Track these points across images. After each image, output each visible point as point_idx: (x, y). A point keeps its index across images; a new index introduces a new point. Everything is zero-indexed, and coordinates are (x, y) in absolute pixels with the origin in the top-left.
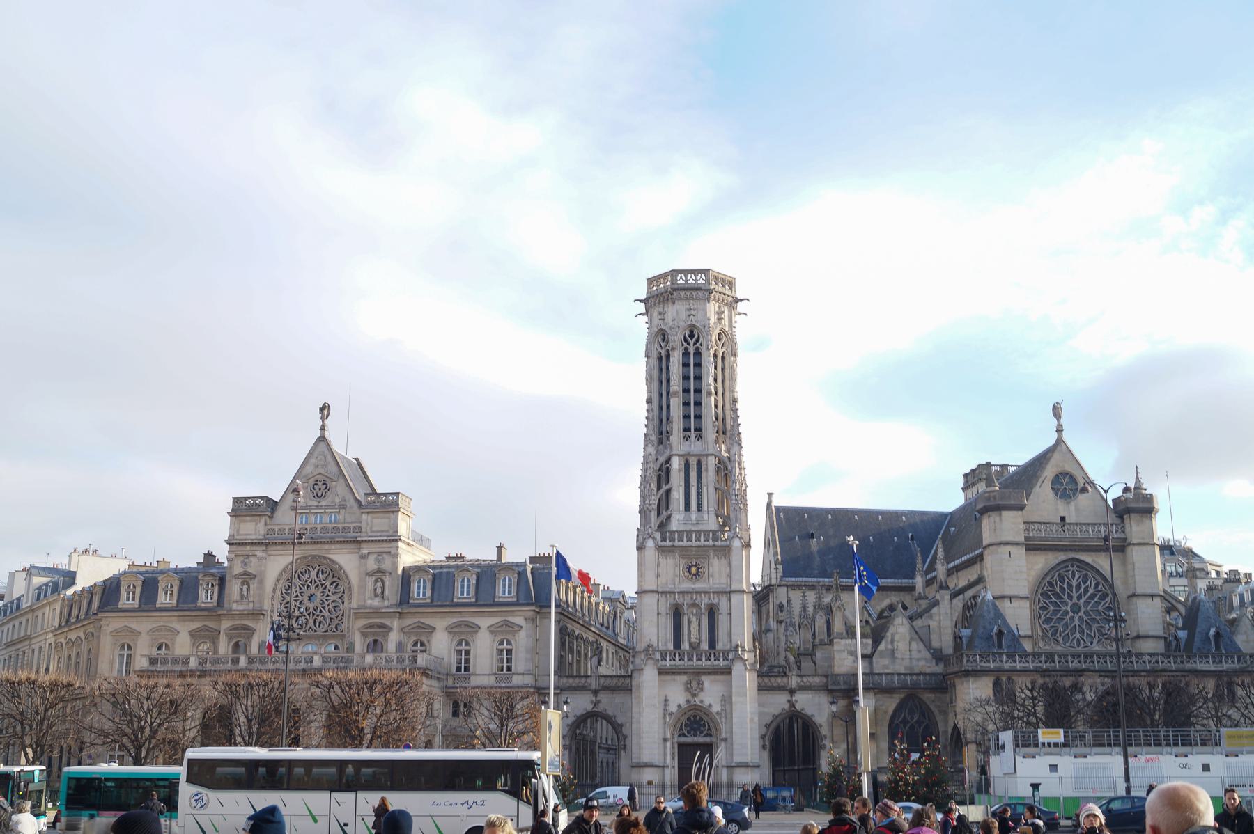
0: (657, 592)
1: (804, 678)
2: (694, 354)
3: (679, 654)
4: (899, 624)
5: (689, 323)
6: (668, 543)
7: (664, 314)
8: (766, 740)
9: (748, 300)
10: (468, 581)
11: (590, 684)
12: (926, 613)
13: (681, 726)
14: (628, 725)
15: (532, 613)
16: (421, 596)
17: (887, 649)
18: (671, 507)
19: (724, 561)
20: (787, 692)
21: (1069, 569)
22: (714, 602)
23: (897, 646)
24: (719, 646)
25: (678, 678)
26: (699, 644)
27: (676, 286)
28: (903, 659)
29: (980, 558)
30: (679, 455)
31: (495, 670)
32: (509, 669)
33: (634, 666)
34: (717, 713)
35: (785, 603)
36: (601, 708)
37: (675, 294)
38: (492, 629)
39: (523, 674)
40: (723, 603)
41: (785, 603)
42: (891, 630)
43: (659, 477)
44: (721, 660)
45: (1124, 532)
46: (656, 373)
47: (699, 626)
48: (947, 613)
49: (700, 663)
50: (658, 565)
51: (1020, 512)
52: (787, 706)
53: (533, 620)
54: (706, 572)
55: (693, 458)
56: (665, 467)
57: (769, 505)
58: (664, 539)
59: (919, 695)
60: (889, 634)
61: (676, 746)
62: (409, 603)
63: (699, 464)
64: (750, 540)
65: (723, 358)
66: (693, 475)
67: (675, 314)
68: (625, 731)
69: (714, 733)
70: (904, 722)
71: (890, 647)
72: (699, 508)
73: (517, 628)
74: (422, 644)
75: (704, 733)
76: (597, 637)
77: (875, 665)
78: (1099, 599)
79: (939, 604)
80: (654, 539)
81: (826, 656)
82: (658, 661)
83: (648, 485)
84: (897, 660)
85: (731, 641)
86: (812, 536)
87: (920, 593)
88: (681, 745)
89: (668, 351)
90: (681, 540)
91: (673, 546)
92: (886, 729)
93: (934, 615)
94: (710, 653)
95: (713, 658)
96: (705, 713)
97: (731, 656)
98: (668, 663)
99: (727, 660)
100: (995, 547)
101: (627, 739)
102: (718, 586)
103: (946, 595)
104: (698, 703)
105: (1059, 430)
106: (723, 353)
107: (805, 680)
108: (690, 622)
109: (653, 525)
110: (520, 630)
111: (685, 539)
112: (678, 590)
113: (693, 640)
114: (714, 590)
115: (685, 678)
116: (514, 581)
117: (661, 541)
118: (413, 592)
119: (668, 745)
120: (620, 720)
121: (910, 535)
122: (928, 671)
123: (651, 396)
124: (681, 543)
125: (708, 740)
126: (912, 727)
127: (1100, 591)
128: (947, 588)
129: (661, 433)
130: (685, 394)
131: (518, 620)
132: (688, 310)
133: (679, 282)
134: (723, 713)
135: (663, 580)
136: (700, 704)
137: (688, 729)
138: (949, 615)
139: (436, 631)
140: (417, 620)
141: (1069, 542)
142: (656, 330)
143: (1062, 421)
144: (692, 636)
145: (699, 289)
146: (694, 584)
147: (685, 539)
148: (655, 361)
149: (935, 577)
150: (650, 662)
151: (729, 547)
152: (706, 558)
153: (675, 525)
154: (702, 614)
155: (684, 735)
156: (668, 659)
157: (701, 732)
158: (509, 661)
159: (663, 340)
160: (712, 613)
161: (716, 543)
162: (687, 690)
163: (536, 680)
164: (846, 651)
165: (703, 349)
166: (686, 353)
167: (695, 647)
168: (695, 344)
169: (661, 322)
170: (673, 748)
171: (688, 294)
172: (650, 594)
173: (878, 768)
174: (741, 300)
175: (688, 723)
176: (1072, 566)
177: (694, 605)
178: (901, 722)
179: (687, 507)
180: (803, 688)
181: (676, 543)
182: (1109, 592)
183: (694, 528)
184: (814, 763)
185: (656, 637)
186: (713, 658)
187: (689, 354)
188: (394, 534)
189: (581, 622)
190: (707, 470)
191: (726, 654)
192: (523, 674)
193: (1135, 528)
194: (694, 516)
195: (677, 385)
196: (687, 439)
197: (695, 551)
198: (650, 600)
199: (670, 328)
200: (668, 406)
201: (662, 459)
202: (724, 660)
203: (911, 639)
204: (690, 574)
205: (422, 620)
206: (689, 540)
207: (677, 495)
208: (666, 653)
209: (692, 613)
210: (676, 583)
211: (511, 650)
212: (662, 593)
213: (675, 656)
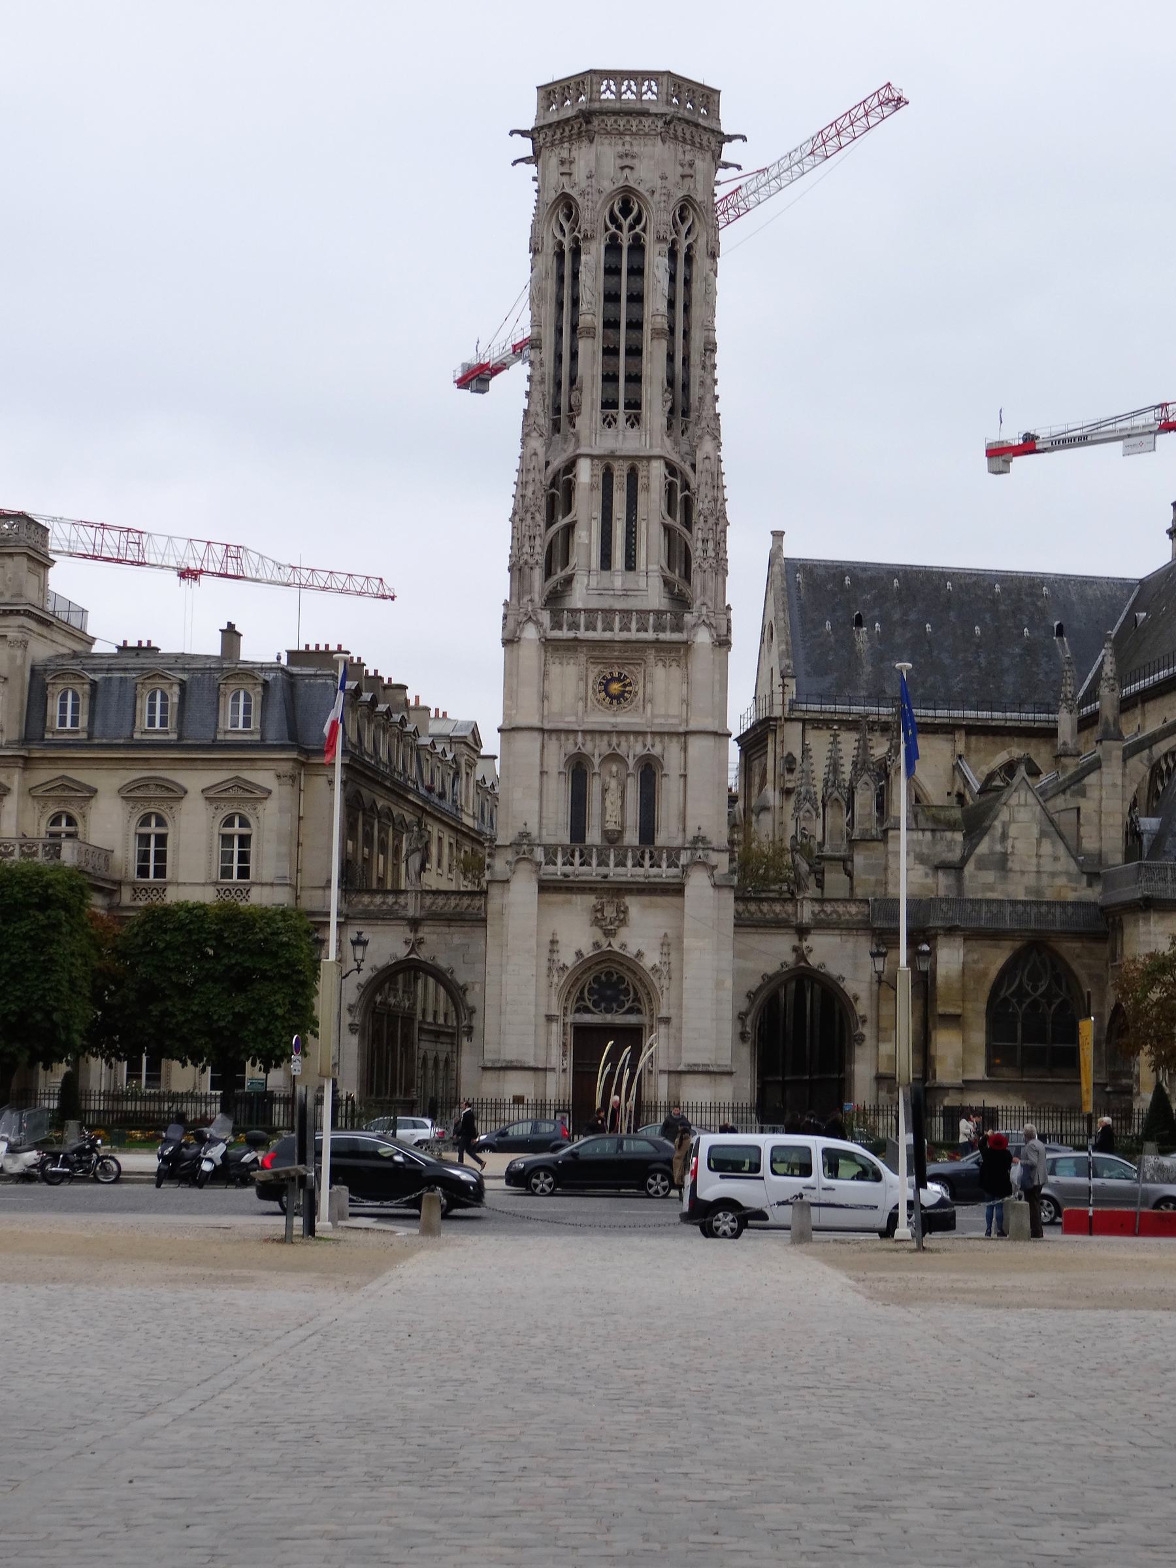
0: (542, 730)
2: (630, 248)
3: (581, 851)
4: (1018, 805)
5: (621, 183)
6: (565, 634)
7: (571, 163)
8: (748, 1022)
9: (744, 138)
10: (164, 697)
11: (405, 907)
12: (1073, 784)
13: (582, 992)
14: (477, 988)
15: (291, 764)
16: (68, 726)
17: (992, 853)
18: (573, 560)
19: (676, 672)
20: (792, 931)
22: (654, 752)
23: (1013, 847)
24: (661, 839)
26: (621, 833)
27: (596, 105)
28: (1023, 872)
30: (592, 457)
31: (216, 875)
32: (244, 873)
33: (492, 874)
34: (654, 968)
35: (797, 754)
36: (423, 954)
37: (596, 122)
38: (211, 794)
39: (272, 884)
41: (797, 754)
42: (1004, 815)
43: (551, 500)
44: (664, 865)
46: (551, 286)
47: (623, 797)
48: (1114, 785)
50: (545, 675)
52: (790, 958)
53: (293, 778)
57: (775, 555)
58: (557, 625)
59: (1052, 944)
60: (997, 824)
61: (570, 1031)
62: (43, 739)
64: (729, 629)
65: (689, 259)
67: (593, 164)
68: (471, 999)
69: (645, 1007)
70: (1020, 993)
72: (630, 564)
73: (256, 795)
74: (71, 821)
75: (627, 1006)
76: (419, 813)
79: (1100, 767)
80: (538, 624)
81: (873, 861)
82: (539, 864)
83: (529, 516)
84: (1011, 875)
85: (684, 830)
86: (859, 622)
87: (1065, 744)
88: (581, 1031)
89: (576, 240)
91: (576, 639)
92: (982, 1006)
93: (1088, 788)
94: (643, 853)
95: (647, 862)
96: (629, 969)
97: (684, 858)
98: (559, 869)
99: (677, 866)
101: (475, 1016)
102: (662, 721)
103: (1116, 749)
104: (616, 948)
106: (690, 247)
107: (828, 908)
108: (605, 791)
109: (536, 597)
110: (266, 798)
111: (599, 625)
112: (581, 728)
113: (611, 826)
114: (654, 729)
115: (592, 900)
116: (256, 700)
117: (552, 629)
118: (53, 717)
119: (556, 1028)
120: (461, 978)
121: (1056, 623)
122: (1071, 896)
123: (539, 333)
124: (590, 635)
125: (632, 1019)
126: (1034, 1005)
128: (1119, 737)
129: (557, 410)
130: (610, 332)
131: (263, 778)
132: (621, 157)
133: (603, 97)
134: (664, 969)
135: (555, 704)
136: (621, 951)
137: (596, 997)
138: (1120, 789)
139: (99, 794)
140: (60, 773)
142: (553, 195)
144: (608, 818)
145: (644, 113)
146: (614, 715)
147: (599, 625)
148: (548, 260)
150: (524, 866)
151: (687, 645)
152: (639, 664)
153: (578, 598)
154: (628, 775)
155: (587, 1010)
156: (560, 860)
157: (621, 1005)
158: (244, 857)
159: (568, 217)
160: (649, 770)
161: (663, 636)
162: (596, 922)
163: (297, 898)
165: (649, 239)
166: (613, 247)
167: (612, 838)
168: (632, 227)
169: (565, 179)
170: (564, 1034)
173: (964, 1081)
174: (730, 138)
175: (596, 986)
178: (1013, 995)
179: (606, 562)
180: (823, 925)
181: (582, 634)
183: (619, 605)
184: (841, 1069)
185: (536, 820)
186: (647, 862)
187: (620, 248)
188: (14, 600)
189: (388, 784)
190: (647, 488)
191: (673, 853)
192: (272, 884)
194: (618, 582)
195: (592, 311)
196: (609, 425)
197: (620, 651)
198: (529, 744)
199: (582, 193)
200: (574, 355)
201: (557, 463)
202: (668, 867)
203: (1043, 834)
204: (608, 694)
205: (71, 774)
206: (608, 627)
207: (587, 538)
208: (556, 850)
210: (580, 714)
211: (248, 837)
213: (573, 856)
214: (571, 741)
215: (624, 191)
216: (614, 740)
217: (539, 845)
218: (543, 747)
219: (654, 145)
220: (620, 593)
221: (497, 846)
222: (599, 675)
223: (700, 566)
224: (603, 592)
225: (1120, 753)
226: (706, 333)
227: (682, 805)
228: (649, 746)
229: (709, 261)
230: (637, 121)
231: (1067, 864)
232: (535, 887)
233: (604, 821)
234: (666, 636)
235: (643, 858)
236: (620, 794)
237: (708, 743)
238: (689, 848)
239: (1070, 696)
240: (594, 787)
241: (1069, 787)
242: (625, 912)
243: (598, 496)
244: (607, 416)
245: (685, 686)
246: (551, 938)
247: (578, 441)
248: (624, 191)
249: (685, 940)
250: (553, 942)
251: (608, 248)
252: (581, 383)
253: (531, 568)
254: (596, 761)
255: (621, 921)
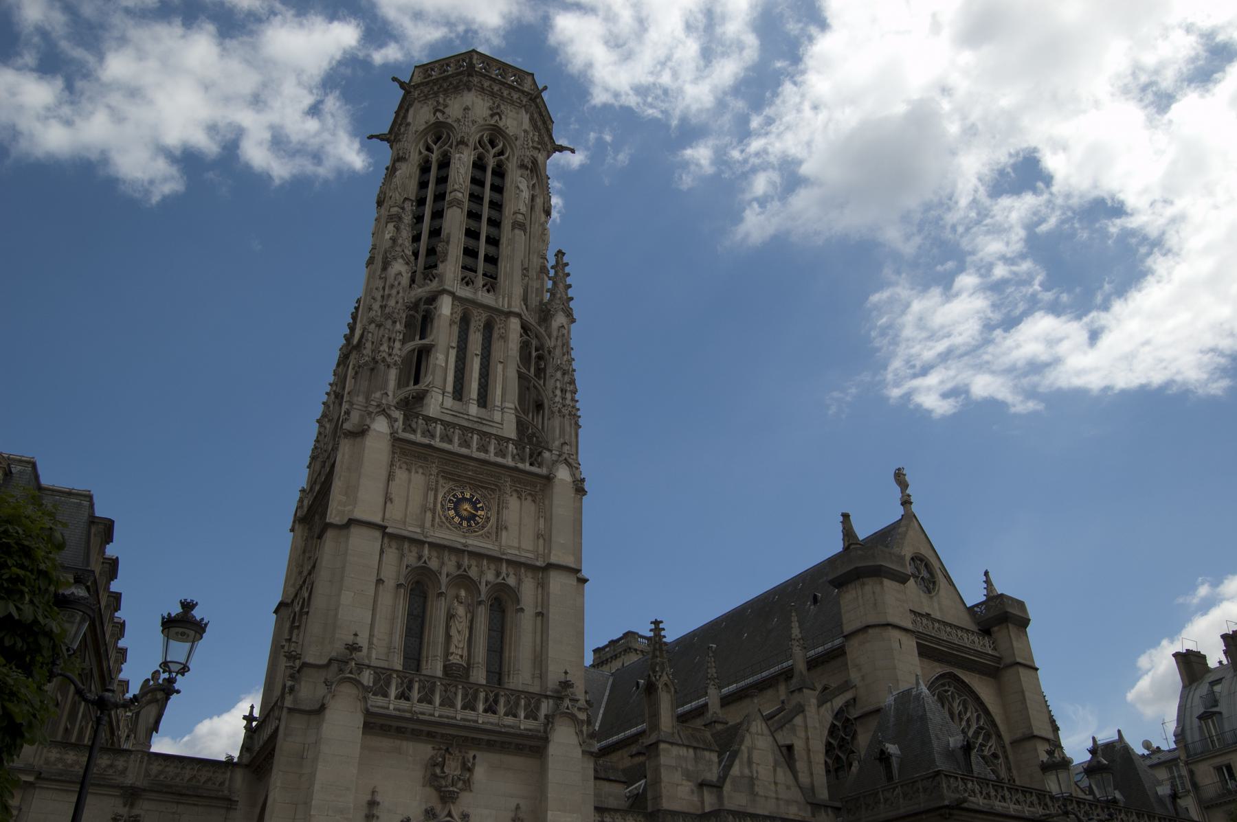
0: (382, 528)
1: (606, 814)
5: (493, 122)
6: (418, 438)
11: (123, 772)
18: (426, 380)
19: (529, 506)
21: (947, 688)
23: (757, 772)
25: (409, 747)
26: (468, 669)
29: (838, 653)
37: (475, 80)
40: (528, 590)
42: (747, 742)
45: (996, 650)
48: (815, 728)
49: (470, 715)
50: (390, 477)
51: (902, 585)
54: (493, 520)
55: (480, 310)
56: (423, 307)
58: (408, 427)
63: (488, 328)
66: (475, 340)
71: (747, 772)
72: (483, 401)
77: (726, 802)
78: (983, 740)
79: (803, 711)
82: (366, 689)
90: (447, 438)
91: (430, 446)
94: (497, 696)
97: (545, 708)
98: (391, 704)
99: (536, 719)
100: (877, 630)
105: (906, 502)
108: (450, 616)
113: (454, 659)
115: (426, 750)
117: (404, 430)
127: (982, 728)
141: (947, 647)
143: (908, 492)
144: (453, 649)
146: (465, 537)
149: (706, 705)
150: (347, 690)
151: (549, 479)
154: (480, 603)
161: (520, 465)
164: (679, 769)
166: (479, 165)
168: (494, 156)
171: (496, 88)
172: (365, 531)
176: (950, 687)
177: (463, 580)
179: (459, 393)
181: (437, 443)
182: (992, 732)
185: (366, 635)
190: (504, 338)
191: (533, 702)
193: (1015, 644)
196: (467, 284)
201: (420, 292)
203: (776, 764)
204: (457, 514)
206: (466, 443)
207: (443, 361)
209: (457, 597)
210: (428, 524)
212: (393, 537)
213: (410, 688)
214: (414, 554)
215: (492, 130)
216: (466, 562)
217: (369, 667)
218: (382, 552)
219: (518, 113)
220: (475, 419)
221: (305, 665)
222: (449, 492)
223: (560, 411)
224: (458, 415)
225: (814, 701)
226: (541, 260)
227: (538, 648)
228: (504, 574)
229: (543, 216)
230: (508, 92)
231: (795, 794)
232: (359, 720)
233: (447, 654)
234: (526, 466)
235: (496, 701)
236: (468, 624)
237: (571, 581)
238: (552, 697)
239: (715, 675)
240: (438, 611)
241: (784, 725)
242: (470, 770)
243: (456, 329)
244: (465, 277)
245: (542, 521)
246: (369, 798)
247: (441, 281)
248: (492, 130)
249: (549, 813)
250: (372, 804)
251: (475, 165)
252: (449, 235)
253: (389, 366)
254: (444, 580)
255: (464, 782)
